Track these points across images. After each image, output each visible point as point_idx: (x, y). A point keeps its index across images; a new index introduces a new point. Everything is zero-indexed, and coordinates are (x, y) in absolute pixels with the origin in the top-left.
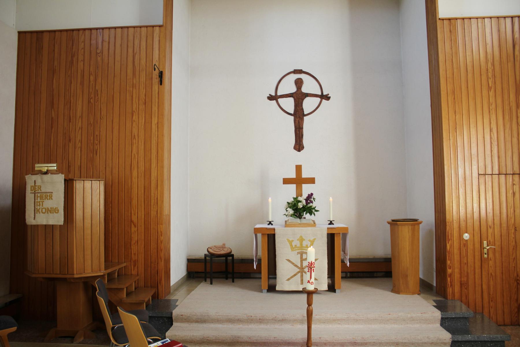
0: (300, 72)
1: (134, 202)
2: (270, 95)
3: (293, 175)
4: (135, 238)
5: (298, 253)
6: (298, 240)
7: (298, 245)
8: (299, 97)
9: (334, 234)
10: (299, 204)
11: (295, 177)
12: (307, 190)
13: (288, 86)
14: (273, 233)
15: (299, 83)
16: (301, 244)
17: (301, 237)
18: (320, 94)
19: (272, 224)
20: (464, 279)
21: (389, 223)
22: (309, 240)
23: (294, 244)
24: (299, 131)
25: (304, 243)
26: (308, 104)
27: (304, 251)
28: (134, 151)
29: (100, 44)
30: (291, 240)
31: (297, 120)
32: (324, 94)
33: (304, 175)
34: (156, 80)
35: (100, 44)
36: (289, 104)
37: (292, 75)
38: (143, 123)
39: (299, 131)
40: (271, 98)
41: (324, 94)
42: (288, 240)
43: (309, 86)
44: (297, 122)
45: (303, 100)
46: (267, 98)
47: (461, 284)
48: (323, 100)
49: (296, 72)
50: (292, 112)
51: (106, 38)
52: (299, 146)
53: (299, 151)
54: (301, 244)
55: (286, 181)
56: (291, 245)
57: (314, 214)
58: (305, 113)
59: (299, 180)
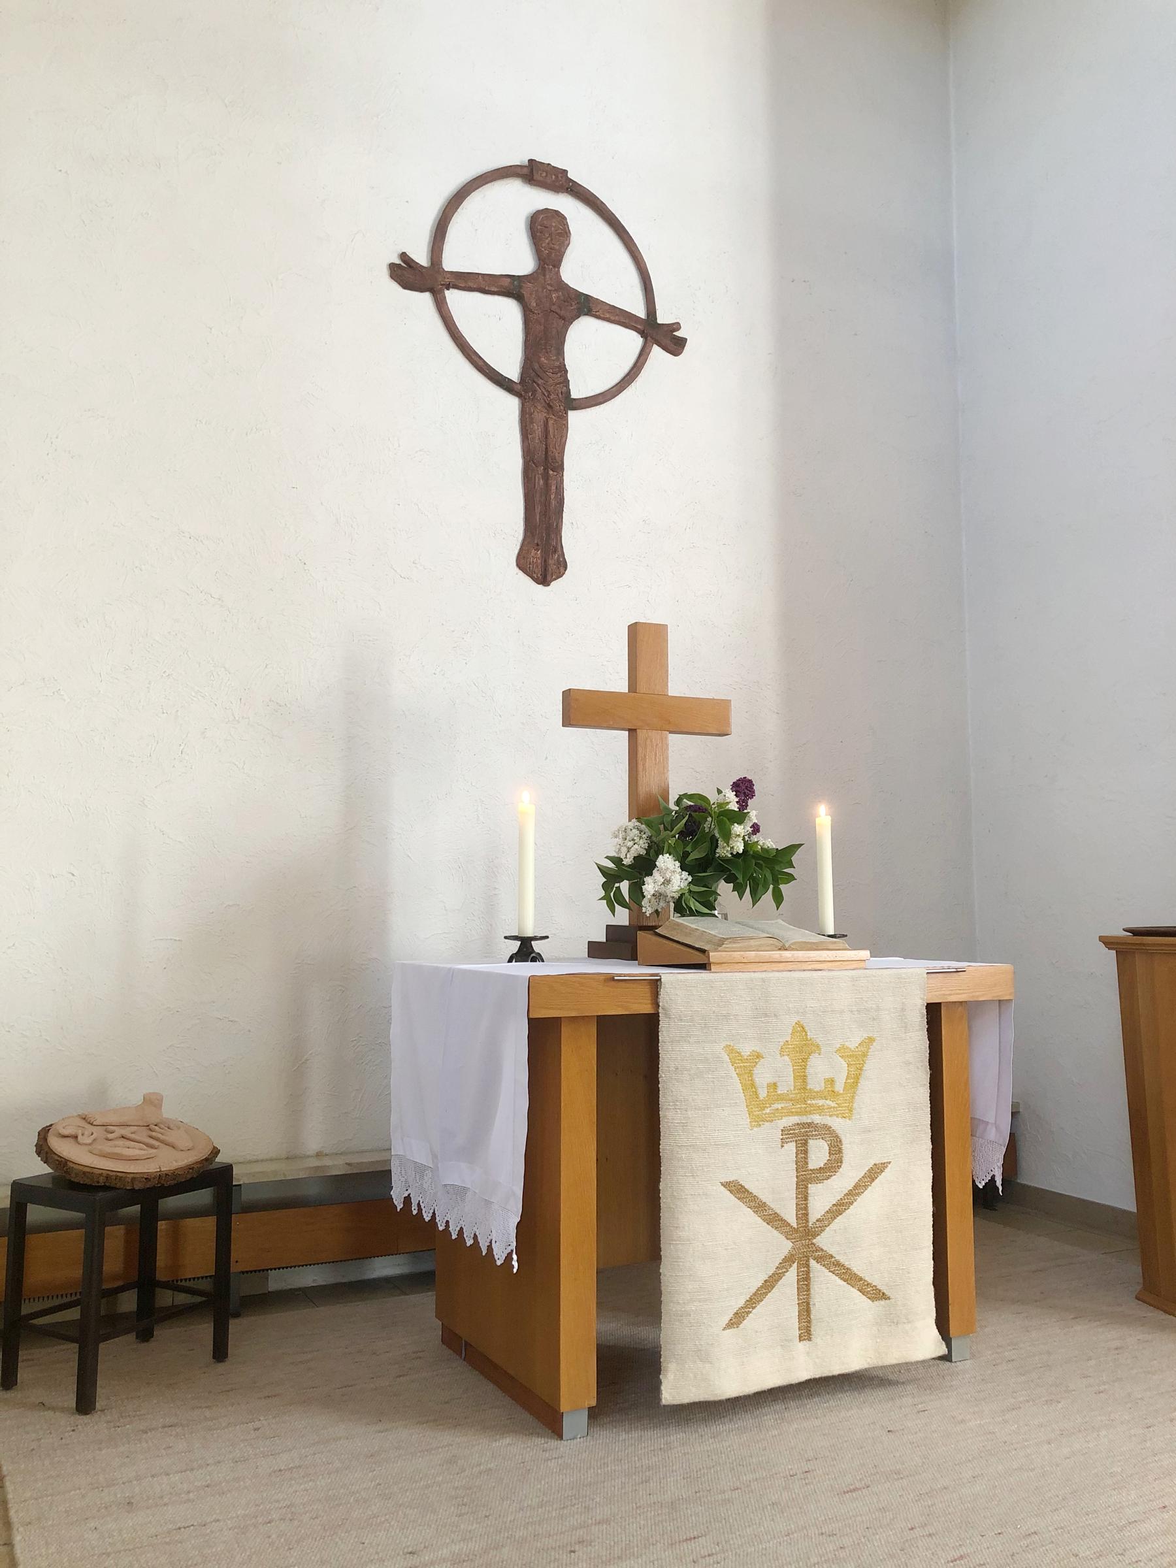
2: (404, 256)
7: (787, 1085)
13: (494, 238)
14: (647, 1009)
15: (547, 234)
16: (802, 1078)
17: (800, 1029)
19: (537, 958)
22: (842, 1051)
23: (763, 1076)
24: (546, 478)
25: (820, 1069)
26: (593, 353)
27: (817, 1119)
30: (746, 1049)
32: (662, 319)
33: (681, 683)
36: (499, 329)
39: (546, 478)
40: (406, 273)
41: (662, 319)
42: (734, 1055)
43: (592, 264)
44: (538, 429)
45: (568, 321)
46: (385, 272)
48: (656, 350)
49: (535, 173)
54: (802, 1078)
55: (580, 709)
56: (750, 1087)
57: (778, 898)
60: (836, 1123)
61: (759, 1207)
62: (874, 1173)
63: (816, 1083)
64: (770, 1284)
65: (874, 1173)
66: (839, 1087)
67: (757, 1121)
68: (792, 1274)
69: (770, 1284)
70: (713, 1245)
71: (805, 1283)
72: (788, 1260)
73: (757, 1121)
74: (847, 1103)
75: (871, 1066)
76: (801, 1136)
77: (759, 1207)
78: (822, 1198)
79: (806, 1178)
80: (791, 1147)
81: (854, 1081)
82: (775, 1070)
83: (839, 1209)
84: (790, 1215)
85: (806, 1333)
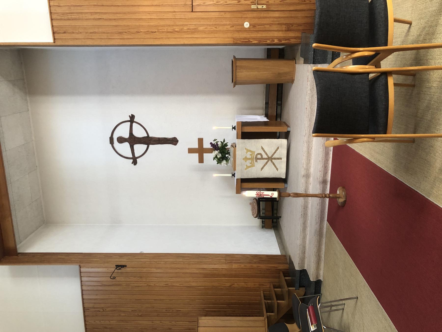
0: (111, 139)
1: (216, 284)
2: (132, 163)
3: (196, 156)
4: (242, 284)
5: (256, 161)
6: (246, 162)
7: (250, 161)
8: (133, 140)
9: (242, 132)
10: (218, 157)
11: (198, 154)
12: (207, 145)
13: (125, 148)
15: (121, 140)
16: (249, 159)
17: (243, 159)
18: (129, 123)
20: (284, 27)
21: (234, 86)
22: (247, 153)
23: (249, 165)
25: (249, 156)
26: (139, 133)
28: (178, 285)
29: (95, 310)
30: (245, 167)
31: (152, 142)
33: (196, 146)
34: (123, 270)
35: (95, 310)
36: (139, 148)
37: (115, 145)
38: (156, 278)
40: (135, 163)
44: (154, 142)
47: (288, 30)
50: (145, 146)
51: (91, 305)
52: (174, 141)
53: (177, 141)
54: (249, 159)
55: (201, 160)
56: (250, 167)
58: (146, 135)
59: (200, 151)
60: (256, 154)
61: (264, 166)
62: (262, 148)
63: (250, 157)
64: (274, 164)
65: (262, 148)
66: (251, 153)
67: (254, 166)
68: (273, 160)
69: (274, 164)
70: (269, 171)
71: (275, 159)
72: (272, 161)
73: (254, 166)
74: (253, 152)
75: (249, 149)
76: (257, 159)
77: (264, 166)
78: (265, 156)
79: (262, 158)
80: (258, 161)
81: (251, 151)
82: (248, 163)
83: (266, 154)
84: (266, 160)
85: (281, 159)
